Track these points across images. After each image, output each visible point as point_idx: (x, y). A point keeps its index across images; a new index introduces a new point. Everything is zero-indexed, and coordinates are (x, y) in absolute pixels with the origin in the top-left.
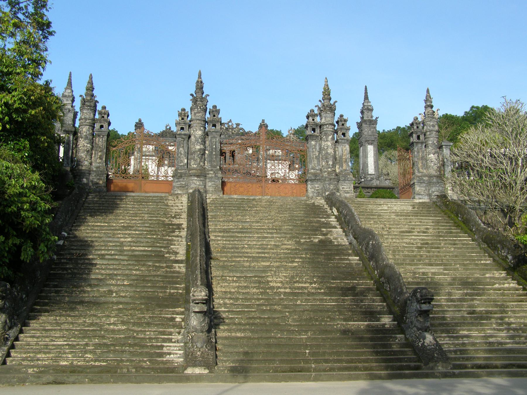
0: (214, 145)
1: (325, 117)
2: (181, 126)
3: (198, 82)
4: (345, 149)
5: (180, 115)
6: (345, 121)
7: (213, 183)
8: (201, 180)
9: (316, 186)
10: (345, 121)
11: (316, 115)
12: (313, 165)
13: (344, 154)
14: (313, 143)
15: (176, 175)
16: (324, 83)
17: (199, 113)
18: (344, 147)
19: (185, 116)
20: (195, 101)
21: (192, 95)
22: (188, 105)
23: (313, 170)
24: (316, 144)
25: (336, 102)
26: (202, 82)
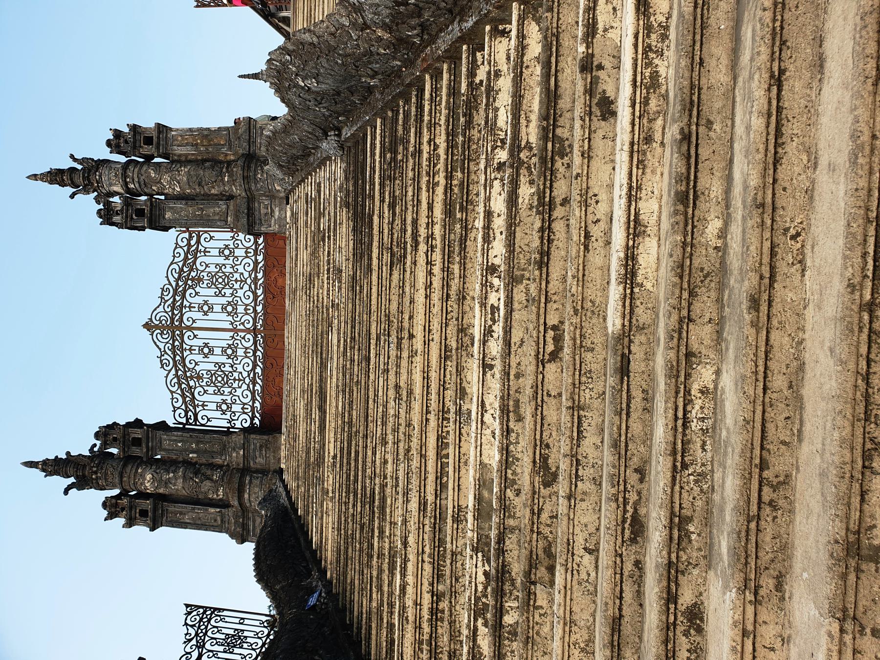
0: (177, 446)
1: (111, 185)
2: (137, 515)
3: (43, 470)
4: (180, 138)
5: (111, 516)
6: (117, 134)
7: (257, 453)
8: (250, 482)
9: (263, 211)
10: (117, 134)
11: (108, 204)
12: (217, 218)
13: (191, 140)
14: (168, 215)
15: (242, 535)
16: (39, 182)
17: (106, 474)
18: (177, 140)
19: (117, 503)
20: (82, 483)
21: (66, 492)
22: (95, 497)
23: (229, 218)
24: (172, 208)
25: (72, 156)
26: (46, 462)
